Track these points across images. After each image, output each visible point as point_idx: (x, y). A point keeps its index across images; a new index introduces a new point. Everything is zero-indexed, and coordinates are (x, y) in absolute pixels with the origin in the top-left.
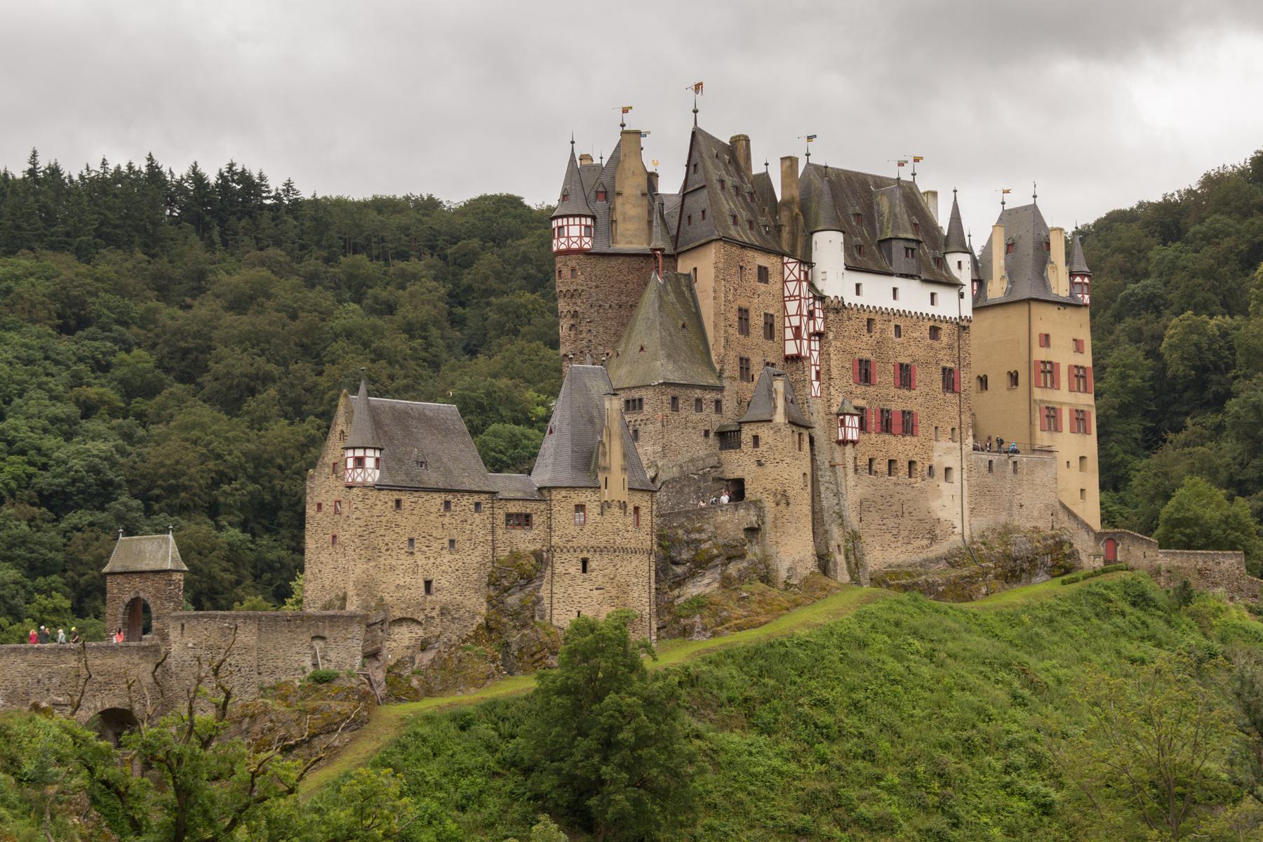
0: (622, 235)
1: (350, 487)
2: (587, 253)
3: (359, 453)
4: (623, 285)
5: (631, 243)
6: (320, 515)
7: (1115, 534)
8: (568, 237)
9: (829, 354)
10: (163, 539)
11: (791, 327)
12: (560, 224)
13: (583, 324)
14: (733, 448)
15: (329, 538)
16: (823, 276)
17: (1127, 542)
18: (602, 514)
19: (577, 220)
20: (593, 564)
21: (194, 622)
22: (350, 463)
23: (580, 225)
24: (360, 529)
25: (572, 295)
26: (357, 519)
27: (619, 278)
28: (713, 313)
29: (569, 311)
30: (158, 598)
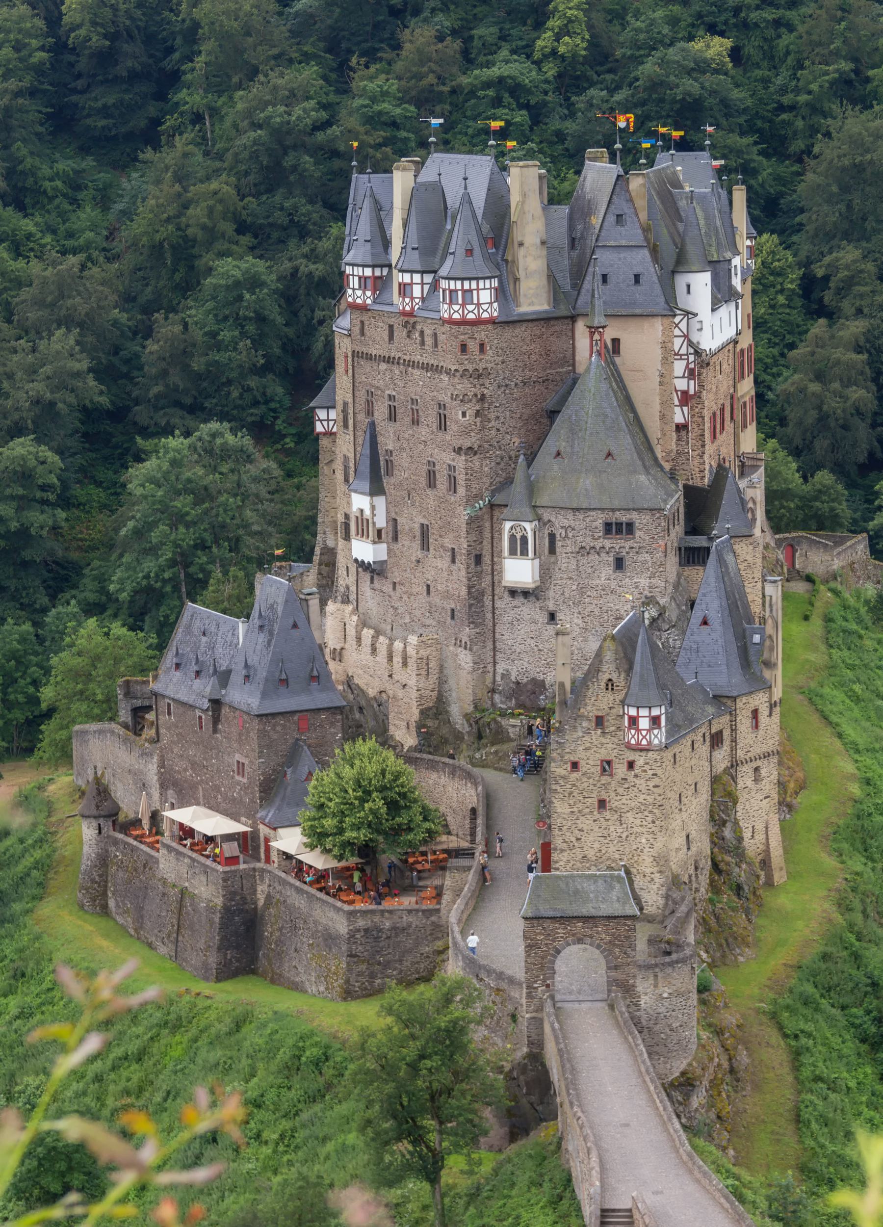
0: (525, 296)
3: (655, 712)
6: (575, 775)
7: (793, 538)
8: (478, 305)
9: (703, 418)
10: (612, 876)
11: (676, 391)
12: (466, 285)
14: (699, 564)
16: (698, 326)
17: (805, 546)
18: (770, 715)
20: (763, 772)
21: (669, 970)
22: (644, 723)
23: (491, 288)
24: (659, 798)
25: (480, 376)
26: (656, 786)
27: (523, 349)
28: (657, 400)
29: (476, 395)
30: (614, 945)
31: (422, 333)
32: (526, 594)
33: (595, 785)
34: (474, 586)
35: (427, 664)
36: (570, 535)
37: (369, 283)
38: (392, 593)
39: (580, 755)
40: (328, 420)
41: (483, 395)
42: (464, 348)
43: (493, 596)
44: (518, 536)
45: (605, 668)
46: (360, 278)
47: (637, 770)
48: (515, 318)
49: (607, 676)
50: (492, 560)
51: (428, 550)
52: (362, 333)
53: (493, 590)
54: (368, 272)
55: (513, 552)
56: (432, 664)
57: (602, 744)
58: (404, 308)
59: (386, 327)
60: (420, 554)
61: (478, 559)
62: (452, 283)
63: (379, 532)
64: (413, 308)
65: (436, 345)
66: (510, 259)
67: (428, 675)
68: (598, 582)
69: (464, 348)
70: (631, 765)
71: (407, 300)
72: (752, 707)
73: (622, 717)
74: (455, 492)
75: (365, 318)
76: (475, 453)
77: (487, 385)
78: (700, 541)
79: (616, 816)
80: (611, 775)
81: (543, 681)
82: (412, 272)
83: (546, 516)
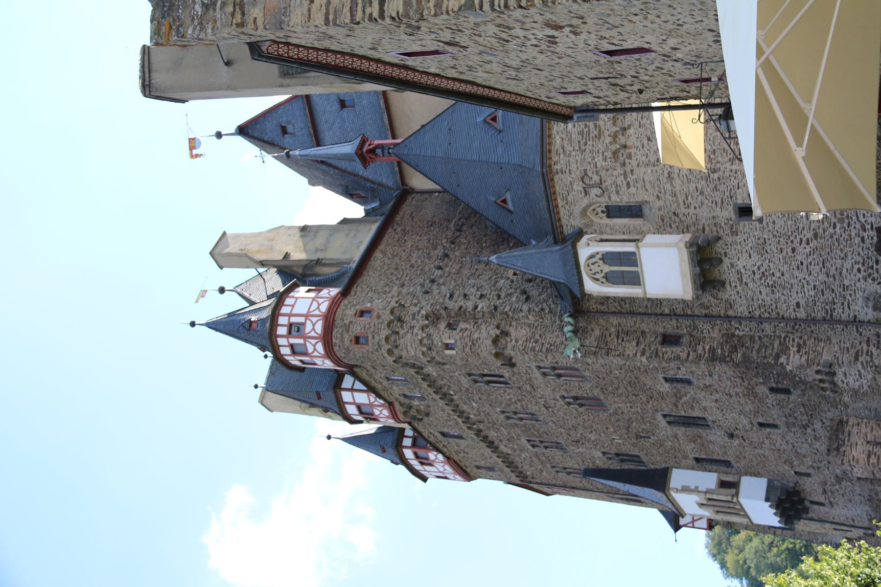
2: (345, 293)
5: (361, 242)
8: (307, 316)
13: (451, 304)
19: (289, 301)
25: (400, 319)
29: (423, 329)
34: (712, 350)
36: (596, 178)
37: (421, 453)
41: (427, 317)
44: (607, 268)
54: (408, 454)
58: (387, 417)
59: (451, 440)
61: (669, 340)
66: (300, 270)
69: (357, 340)
71: (376, 412)
76: (506, 334)
77: (415, 309)
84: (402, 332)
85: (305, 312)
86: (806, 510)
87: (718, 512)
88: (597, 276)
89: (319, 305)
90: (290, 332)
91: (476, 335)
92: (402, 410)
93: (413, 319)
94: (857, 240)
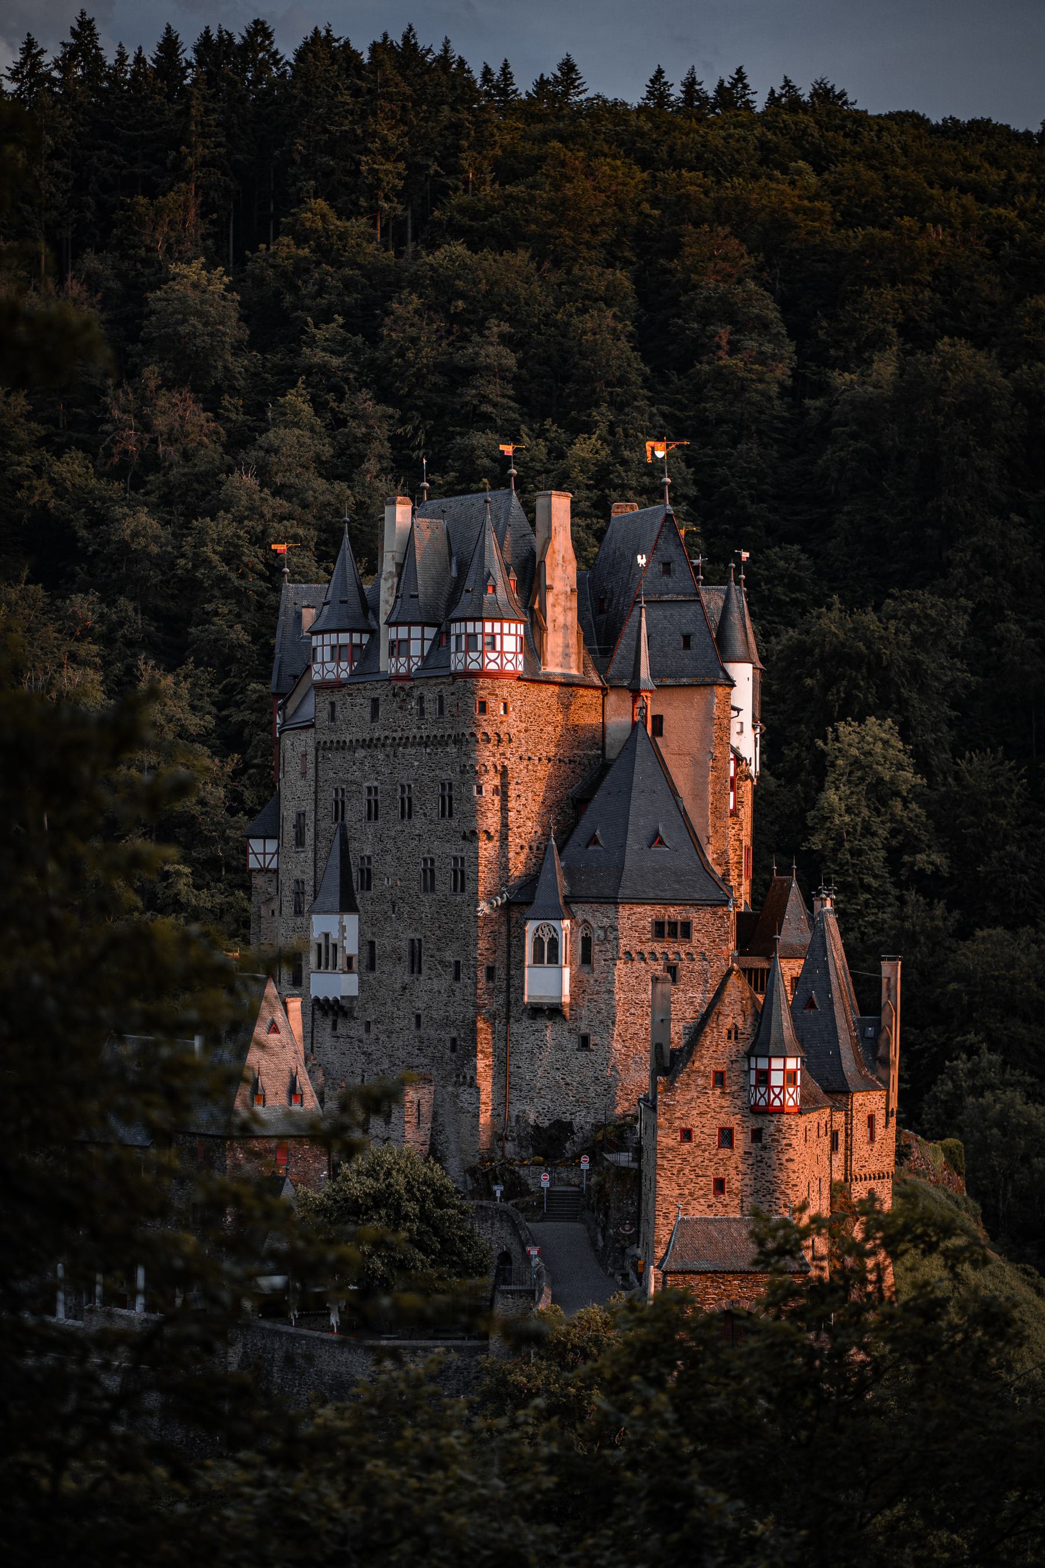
0: (553, 653)
1: (756, 1111)
4: (550, 728)
6: (687, 1146)
8: (502, 653)
15: (709, 1183)
23: (516, 635)
27: (549, 718)
31: (421, 699)
32: (553, 1012)
33: (710, 1160)
35: (419, 1110)
37: (346, 652)
38: (365, 1036)
39: (693, 1122)
40: (265, 854)
41: (504, 767)
42: (483, 707)
43: (508, 1018)
44: (546, 940)
45: (727, 1010)
46: (333, 647)
47: (766, 1140)
48: (542, 678)
49: (728, 1022)
50: (508, 974)
51: (420, 972)
52: (333, 718)
53: (508, 1011)
54: (344, 638)
55: (538, 959)
56: (424, 1109)
57: (723, 1107)
58: (397, 670)
59: (367, 703)
60: (407, 978)
61: (490, 972)
62: (470, 625)
63: (350, 959)
64: (410, 669)
65: (441, 711)
67: (419, 1123)
68: (644, 996)
70: (757, 1135)
71: (402, 660)
72: (868, 1110)
73: (747, 1073)
74: (463, 890)
75: (336, 697)
77: (508, 755)
78: (758, 963)
79: (737, 1202)
80: (731, 1145)
81: (570, 1124)
82: (410, 624)
83: (580, 918)
84: (490, 746)
85: (505, 650)
86: (325, 1014)
87: (319, 946)
88: (540, 932)
89: (510, 661)
90: (488, 635)
91: (489, 815)
92: (407, 687)
93: (501, 754)
94: (564, 1110)
